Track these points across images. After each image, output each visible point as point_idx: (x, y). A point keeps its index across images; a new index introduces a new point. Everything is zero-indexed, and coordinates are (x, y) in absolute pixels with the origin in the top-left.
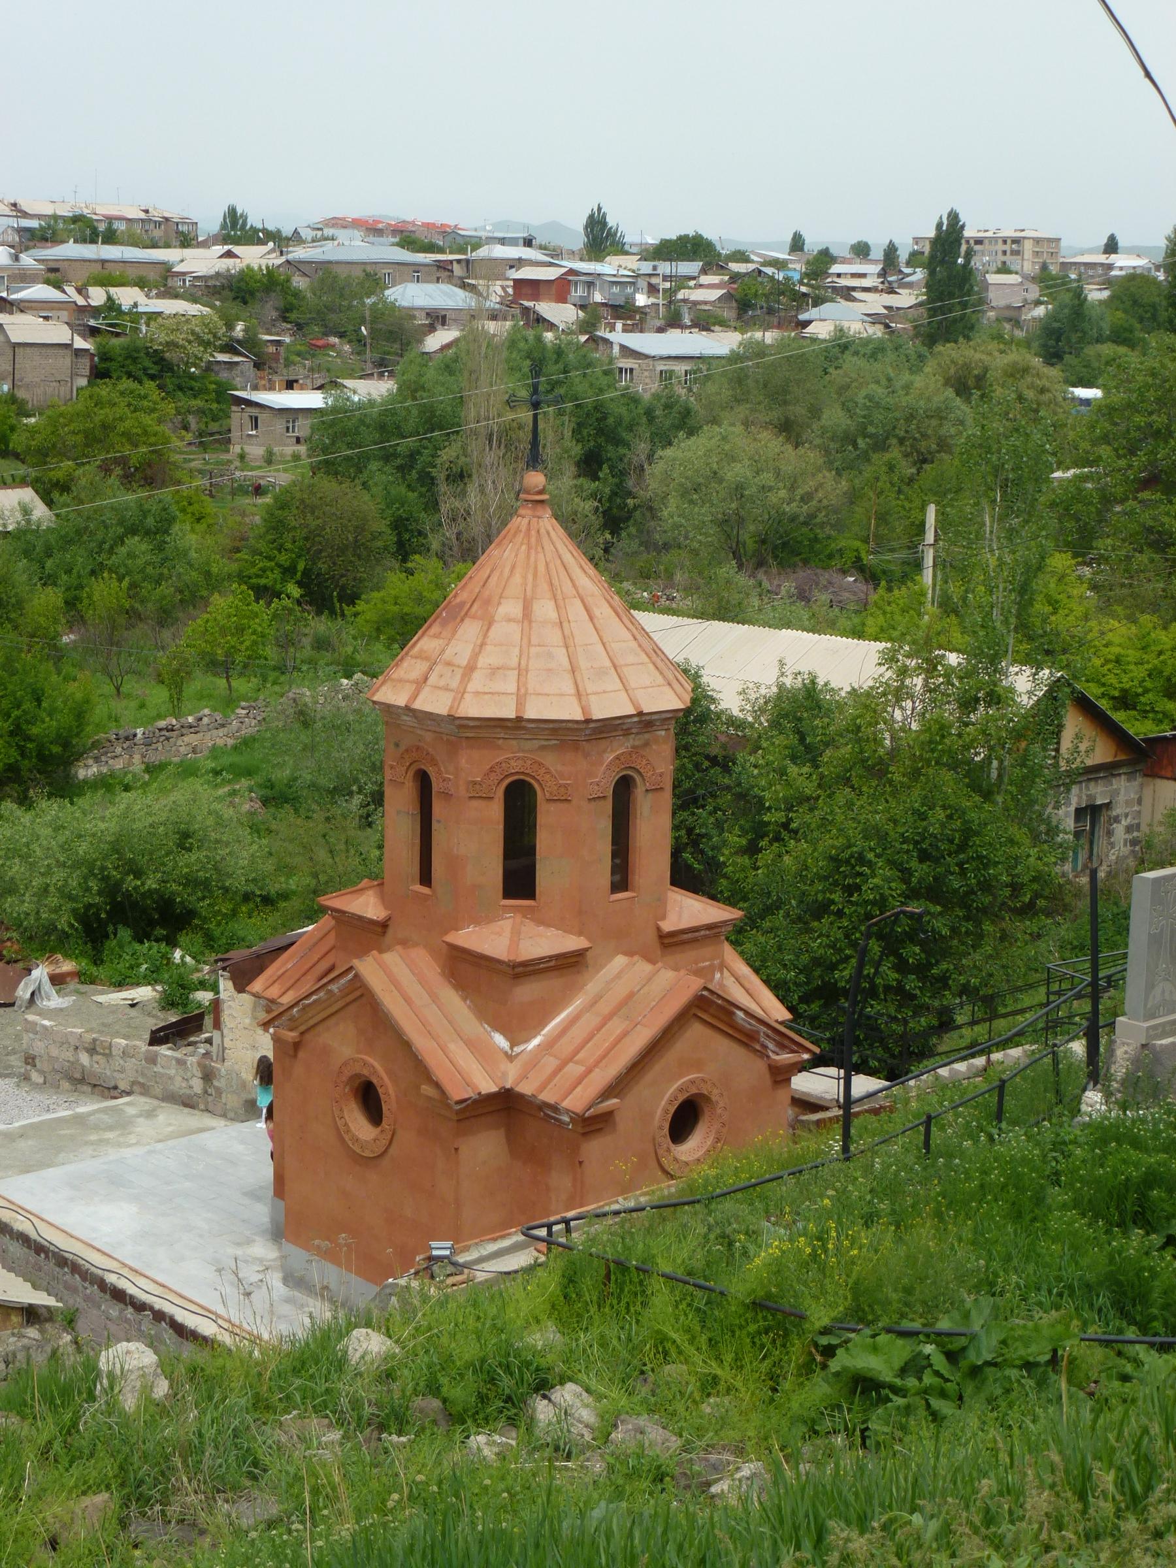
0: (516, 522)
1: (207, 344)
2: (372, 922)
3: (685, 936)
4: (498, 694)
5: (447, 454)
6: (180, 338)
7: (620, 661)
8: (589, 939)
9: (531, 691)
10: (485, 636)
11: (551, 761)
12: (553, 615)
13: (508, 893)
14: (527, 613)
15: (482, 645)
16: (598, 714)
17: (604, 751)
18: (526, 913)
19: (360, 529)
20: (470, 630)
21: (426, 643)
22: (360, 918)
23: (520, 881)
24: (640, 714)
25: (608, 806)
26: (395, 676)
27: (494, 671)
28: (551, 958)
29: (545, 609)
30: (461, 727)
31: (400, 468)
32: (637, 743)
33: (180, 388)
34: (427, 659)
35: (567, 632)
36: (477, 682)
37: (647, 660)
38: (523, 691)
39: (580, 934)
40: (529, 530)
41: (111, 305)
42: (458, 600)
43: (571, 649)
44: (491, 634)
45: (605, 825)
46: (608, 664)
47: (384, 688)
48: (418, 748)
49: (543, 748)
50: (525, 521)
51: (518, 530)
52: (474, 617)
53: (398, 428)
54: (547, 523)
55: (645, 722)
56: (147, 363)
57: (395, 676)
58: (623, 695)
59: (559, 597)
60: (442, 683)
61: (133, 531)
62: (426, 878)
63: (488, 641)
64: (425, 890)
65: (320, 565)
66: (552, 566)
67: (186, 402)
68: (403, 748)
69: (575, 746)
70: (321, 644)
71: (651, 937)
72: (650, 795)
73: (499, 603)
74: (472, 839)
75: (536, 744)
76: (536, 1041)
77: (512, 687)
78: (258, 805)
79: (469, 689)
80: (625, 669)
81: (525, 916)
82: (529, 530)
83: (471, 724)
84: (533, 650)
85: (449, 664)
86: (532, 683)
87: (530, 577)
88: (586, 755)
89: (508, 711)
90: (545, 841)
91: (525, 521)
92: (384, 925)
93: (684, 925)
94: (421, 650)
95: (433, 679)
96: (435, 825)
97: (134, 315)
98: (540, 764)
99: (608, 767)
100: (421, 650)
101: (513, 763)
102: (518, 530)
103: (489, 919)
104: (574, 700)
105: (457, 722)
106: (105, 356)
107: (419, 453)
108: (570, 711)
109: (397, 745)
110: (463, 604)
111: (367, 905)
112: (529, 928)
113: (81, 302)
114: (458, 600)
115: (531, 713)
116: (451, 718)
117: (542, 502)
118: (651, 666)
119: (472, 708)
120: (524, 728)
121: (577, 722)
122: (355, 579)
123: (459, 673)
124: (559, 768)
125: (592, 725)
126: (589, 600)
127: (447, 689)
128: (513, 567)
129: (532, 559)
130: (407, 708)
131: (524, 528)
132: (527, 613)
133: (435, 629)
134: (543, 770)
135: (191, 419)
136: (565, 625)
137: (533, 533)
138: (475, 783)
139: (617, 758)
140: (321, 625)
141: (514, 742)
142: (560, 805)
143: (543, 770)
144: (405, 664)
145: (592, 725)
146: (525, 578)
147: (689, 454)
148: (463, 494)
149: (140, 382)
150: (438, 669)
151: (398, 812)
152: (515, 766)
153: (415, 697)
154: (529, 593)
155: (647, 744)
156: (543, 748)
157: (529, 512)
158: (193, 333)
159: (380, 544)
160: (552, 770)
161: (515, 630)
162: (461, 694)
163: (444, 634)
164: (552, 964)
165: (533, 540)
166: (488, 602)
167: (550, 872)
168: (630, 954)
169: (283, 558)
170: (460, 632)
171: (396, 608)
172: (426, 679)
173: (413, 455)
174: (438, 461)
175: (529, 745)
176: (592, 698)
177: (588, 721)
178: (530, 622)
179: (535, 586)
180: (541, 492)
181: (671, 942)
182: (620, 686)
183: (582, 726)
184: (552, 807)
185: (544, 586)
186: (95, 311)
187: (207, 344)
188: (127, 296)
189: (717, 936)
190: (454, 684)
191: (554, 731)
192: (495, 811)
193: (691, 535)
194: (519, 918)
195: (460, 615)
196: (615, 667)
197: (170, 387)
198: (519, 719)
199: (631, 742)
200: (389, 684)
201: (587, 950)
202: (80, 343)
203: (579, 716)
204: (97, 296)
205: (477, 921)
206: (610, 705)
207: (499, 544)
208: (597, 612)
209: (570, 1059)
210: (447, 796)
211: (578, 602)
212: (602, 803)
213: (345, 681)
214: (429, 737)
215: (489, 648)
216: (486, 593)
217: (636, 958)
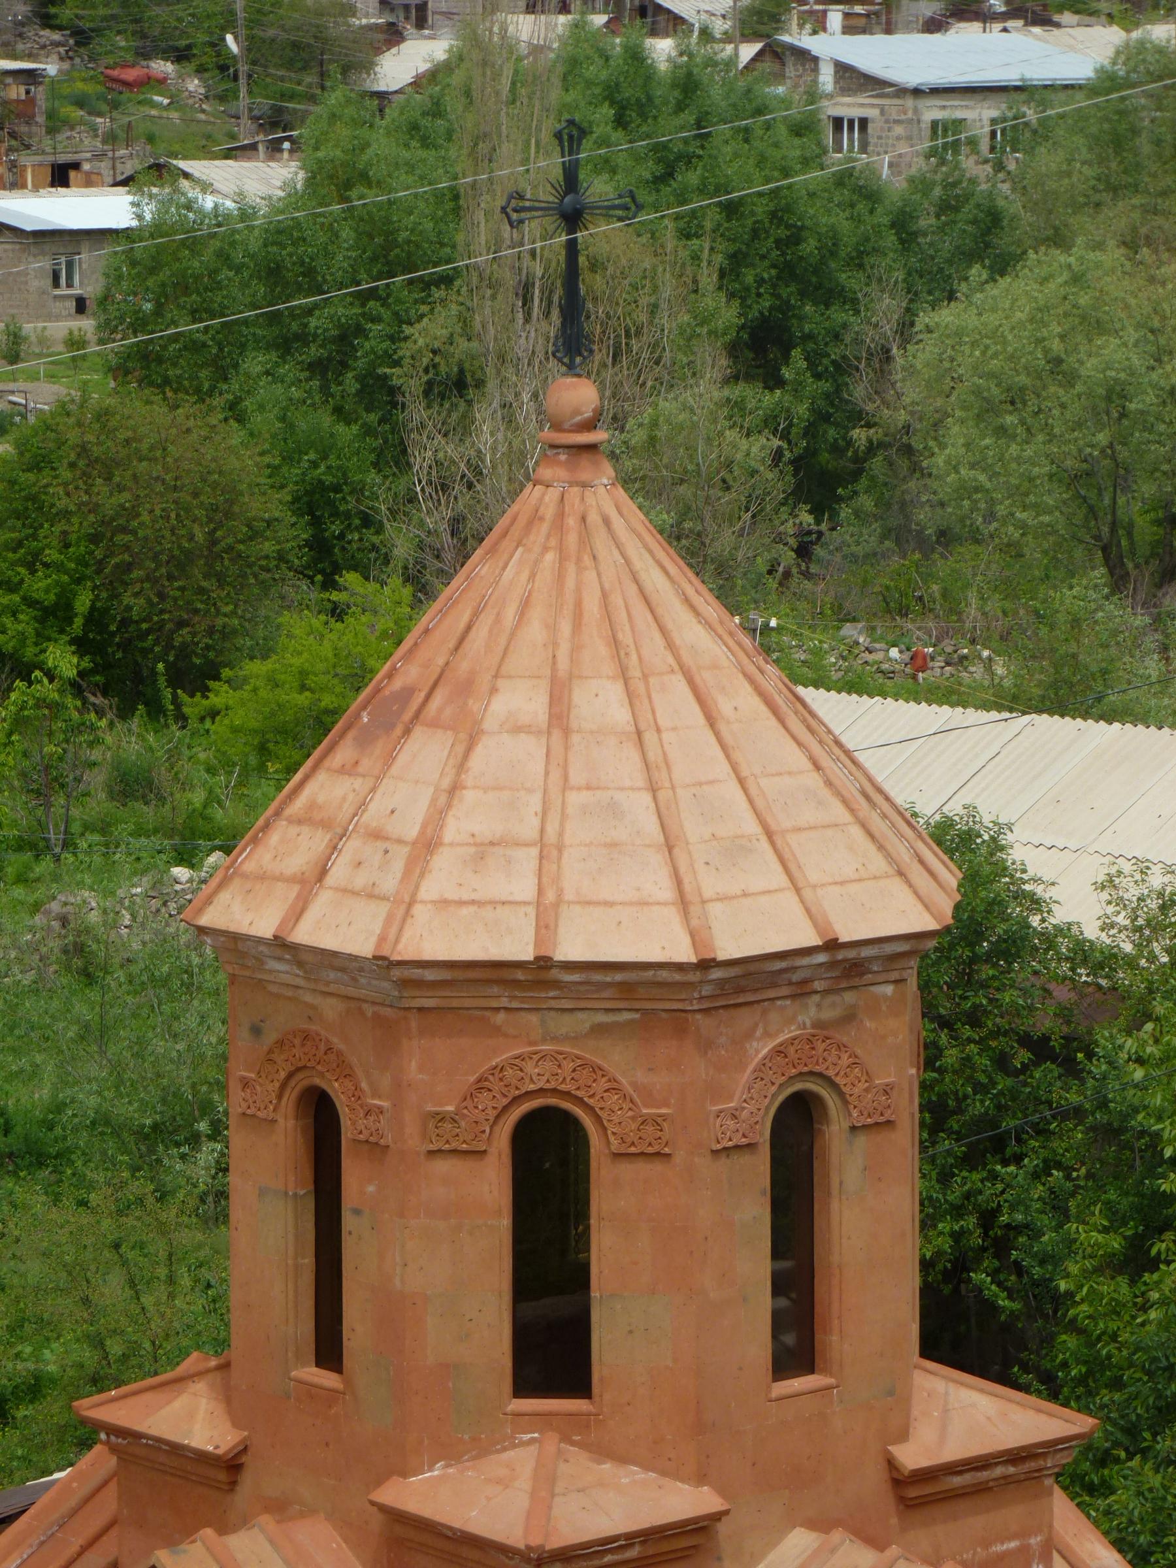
0: (532, 495)
2: (202, 1457)
3: (957, 1481)
4: (494, 903)
5: (429, 331)
7: (781, 821)
8: (722, 1492)
9: (569, 895)
10: (461, 767)
11: (622, 1061)
12: (621, 715)
13: (523, 1387)
14: (559, 716)
15: (455, 789)
16: (729, 948)
17: (749, 1035)
19: (221, 515)
20: (425, 754)
21: (325, 787)
22: (176, 1449)
23: (553, 1352)
24: (832, 945)
25: (760, 1165)
26: (249, 867)
27: (483, 851)
28: (631, 1538)
29: (601, 702)
30: (405, 983)
31: (317, 368)
32: (828, 1014)
34: (326, 824)
35: (653, 754)
36: (443, 878)
37: (847, 817)
38: (550, 896)
39: (701, 1478)
40: (561, 515)
42: (397, 684)
43: (662, 795)
44: (477, 761)
45: (756, 1213)
46: (751, 826)
47: (224, 897)
48: (307, 1037)
49: (599, 1030)
50: (552, 495)
51: (535, 517)
52: (435, 724)
53: (310, 272)
54: (604, 497)
55: (845, 965)
57: (249, 867)
58: (790, 897)
59: (635, 673)
60: (360, 880)
62: (329, 1349)
63: (468, 779)
64: (328, 1379)
65: (127, 599)
66: (617, 600)
68: (270, 1037)
69: (678, 1022)
70: (131, 786)
71: (874, 1479)
72: (862, 1140)
73: (494, 690)
74: (439, 1252)
75: (585, 1021)
77: (523, 887)
79: (423, 894)
80: (793, 840)
81: (566, 1439)
82: (561, 515)
83: (430, 975)
84: (574, 798)
85: (377, 835)
86: (575, 875)
87: (566, 628)
88: (706, 1046)
89: (518, 946)
91: (552, 495)
92: (232, 1466)
93: (952, 1452)
94: (312, 805)
95: (338, 873)
96: (348, 1221)
98: (596, 1069)
100: (312, 805)
101: (530, 1068)
102: (535, 517)
103: (482, 1448)
104: (672, 915)
105: (396, 973)
107: (360, 331)
108: (662, 942)
109: (256, 1031)
110: (408, 693)
111: (192, 1418)
112: (577, 1465)
114: (397, 684)
115: (572, 947)
116: (383, 964)
117: (592, 448)
118: (856, 832)
119: (434, 940)
120: (556, 984)
121: (680, 967)
122: (211, 631)
123: (400, 856)
124: (641, 1077)
125: (716, 974)
126: (706, 678)
127: (371, 894)
128: (525, 605)
129: (570, 583)
130: (280, 944)
131: (549, 511)
132: (559, 716)
133: (344, 753)
134: (603, 1084)
136: (650, 737)
137: (571, 522)
138: (441, 1118)
139: (779, 1051)
140: (128, 741)
141: (534, 1018)
142: (643, 1168)
143: (603, 1084)
144: (274, 838)
145: (716, 974)
146: (552, 628)
147: (992, 319)
148: (464, 429)
150: (351, 847)
151: (262, 1192)
152: (537, 1075)
153: (297, 913)
154: (563, 664)
155: (849, 1017)
156: (599, 1030)
157: (561, 473)
159: (269, 547)
160: (624, 1082)
161: (528, 755)
162: (404, 906)
163: (366, 764)
165: (572, 539)
166: (466, 688)
167: (627, 1327)
168: (820, 1524)
169: (41, 586)
170: (403, 758)
171: (304, 699)
172: (323, 872)
173: (347, 337)
174: (405, 351)
175: (566, 1024)
176: (716, 910)
177: (705, 965)
178: (567, 732)
179: (576, 649)
180: (590, 425)
181: (922, 1494)
182: (779, 878)
184: (627, 1170)
185: (597, 648)
189: (1035, 1477)
190: (389, 883)
191: (627, 989)
192: (491, 1184)
193: (1001, 510)
194: (552, 1442)
195: (402, 719)
196: (770, 835)
198: (543, 963)
199: (809, 1013)
200: (237, 882)
201: (717, 1517)
203: (684, 953)
205: (450, 1452)
206: (759, 923)
207: (493, 550)
208: (725, 706)
210: (375, 1149)
212: (745, 1159)
213: (181, 872)
214: (331, 1009)
215: (469, 795)
216: (463, 666)
217: (837, 1535)
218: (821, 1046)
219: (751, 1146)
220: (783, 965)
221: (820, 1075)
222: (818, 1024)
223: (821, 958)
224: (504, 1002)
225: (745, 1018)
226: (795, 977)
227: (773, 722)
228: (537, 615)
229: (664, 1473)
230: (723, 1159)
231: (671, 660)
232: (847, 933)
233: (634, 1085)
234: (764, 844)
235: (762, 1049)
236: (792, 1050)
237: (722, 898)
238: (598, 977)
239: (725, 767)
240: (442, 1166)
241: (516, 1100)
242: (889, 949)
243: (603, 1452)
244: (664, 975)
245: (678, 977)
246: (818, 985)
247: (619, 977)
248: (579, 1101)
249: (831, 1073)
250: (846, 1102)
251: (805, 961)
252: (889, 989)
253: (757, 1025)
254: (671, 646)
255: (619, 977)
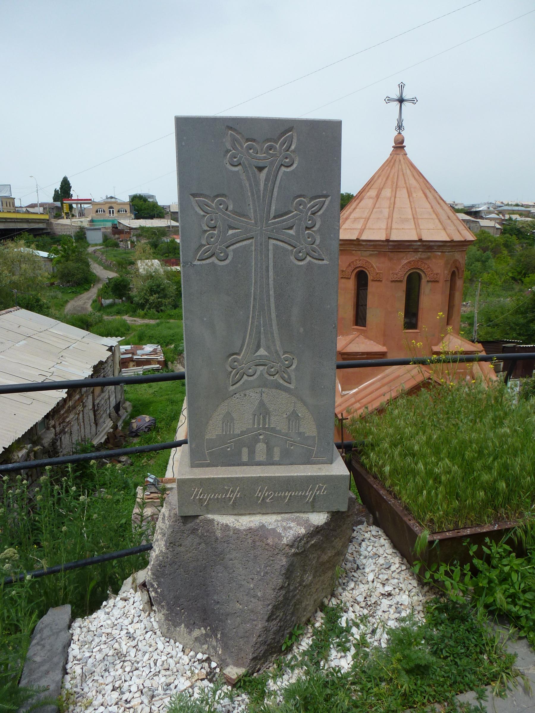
1: (531, 227)
4: (353, 229)
6: (524, 225)
14: (378, 196)
17: (402, 258)
18: (362, 332)
23: (360, 318)
24: (420, 240)
25: (403, 286)
27: (356, 219)
28: (363, 353)
29: (387, 193)
32: (423, 257)
33: (523, 238)
39: (384, 345)
41: (510, 219)
46: (410, 216)
55: (427, 247)
56: (515, 231)
61: (478, 260)
67: (523, 240)
72: (430, 284)
76: (354, 391)
78: (467, 325)
80: (420, 221)
88: (390, 259)
90: (372, 300)
97: (516, 221)
99: (403, 267)
106: (505, 230)
113: (503, 218)
118: (437, 221)
120: (361, 245)
132: (378, 196)
135: (524, 245)
139: (409, 262)
141: (359, 252)
145: (391, 243)
149: (512, 236)
152: (359, 264)
155: (428, 258)
156: (371, 255)
158: (528, 224)
160: (376, 265)
164: (365, 356)
167: (374, 315)
169: (519, 270)
183: (386, 243)
184: (375, 283)
186: (506, 220)
187: (531, 227)
188: (514, 217)
191: (375, 246)
192: (351, 284)
196: (414, 218)
197: (520, 237)
199: (418, 256)
202: (498, 226)
204: (507, 217)
209: (359, 401)
211: (405, 191)
212: (399, 284)
218: (420, 263)
219: (401, 281)
220: (409, 244)
221: (419, 269)
222: (420, 258)
223: (419, 243)
224: (354, 249)
225: (402, 255)
226: (414, 247)
227: (425, 199)
228: (380, 178)
229: (377, 343)
230: (393, 284)
231: (405, 186)
232: (424, 238)
233: (376, 266)
234: (412, 220)
235: (405, 262)
236: (412, 263)
237: (396, 229)
238: (368, 243)
239: (409, 205)
240: (343, 280)
241: (355, 268)
242: (437, 244)
243: (367, 337)
244: (380, 243)
245: (383, 243)
246: (420, 250)
247: (372, 243)
248: (366, 269)
249: (422, 269)
250: (426, 276)
251: (415, 244)
252: (440, 253)
253: (404, 257)
254: (406, 183)
255: (372, 243)
